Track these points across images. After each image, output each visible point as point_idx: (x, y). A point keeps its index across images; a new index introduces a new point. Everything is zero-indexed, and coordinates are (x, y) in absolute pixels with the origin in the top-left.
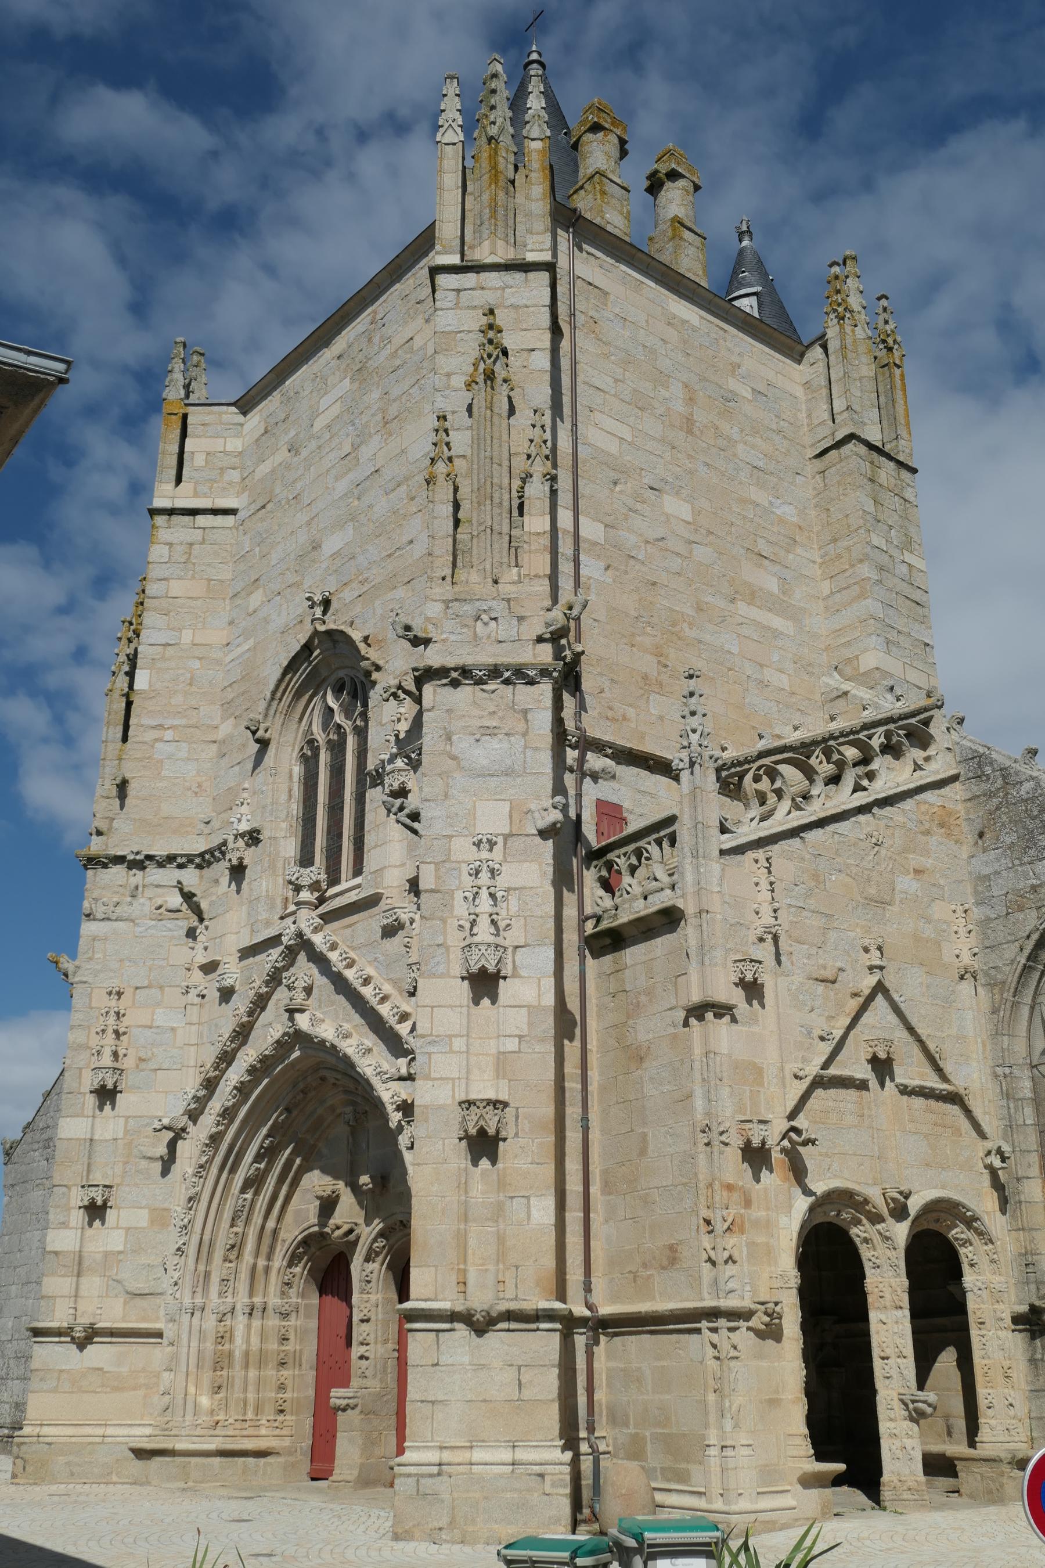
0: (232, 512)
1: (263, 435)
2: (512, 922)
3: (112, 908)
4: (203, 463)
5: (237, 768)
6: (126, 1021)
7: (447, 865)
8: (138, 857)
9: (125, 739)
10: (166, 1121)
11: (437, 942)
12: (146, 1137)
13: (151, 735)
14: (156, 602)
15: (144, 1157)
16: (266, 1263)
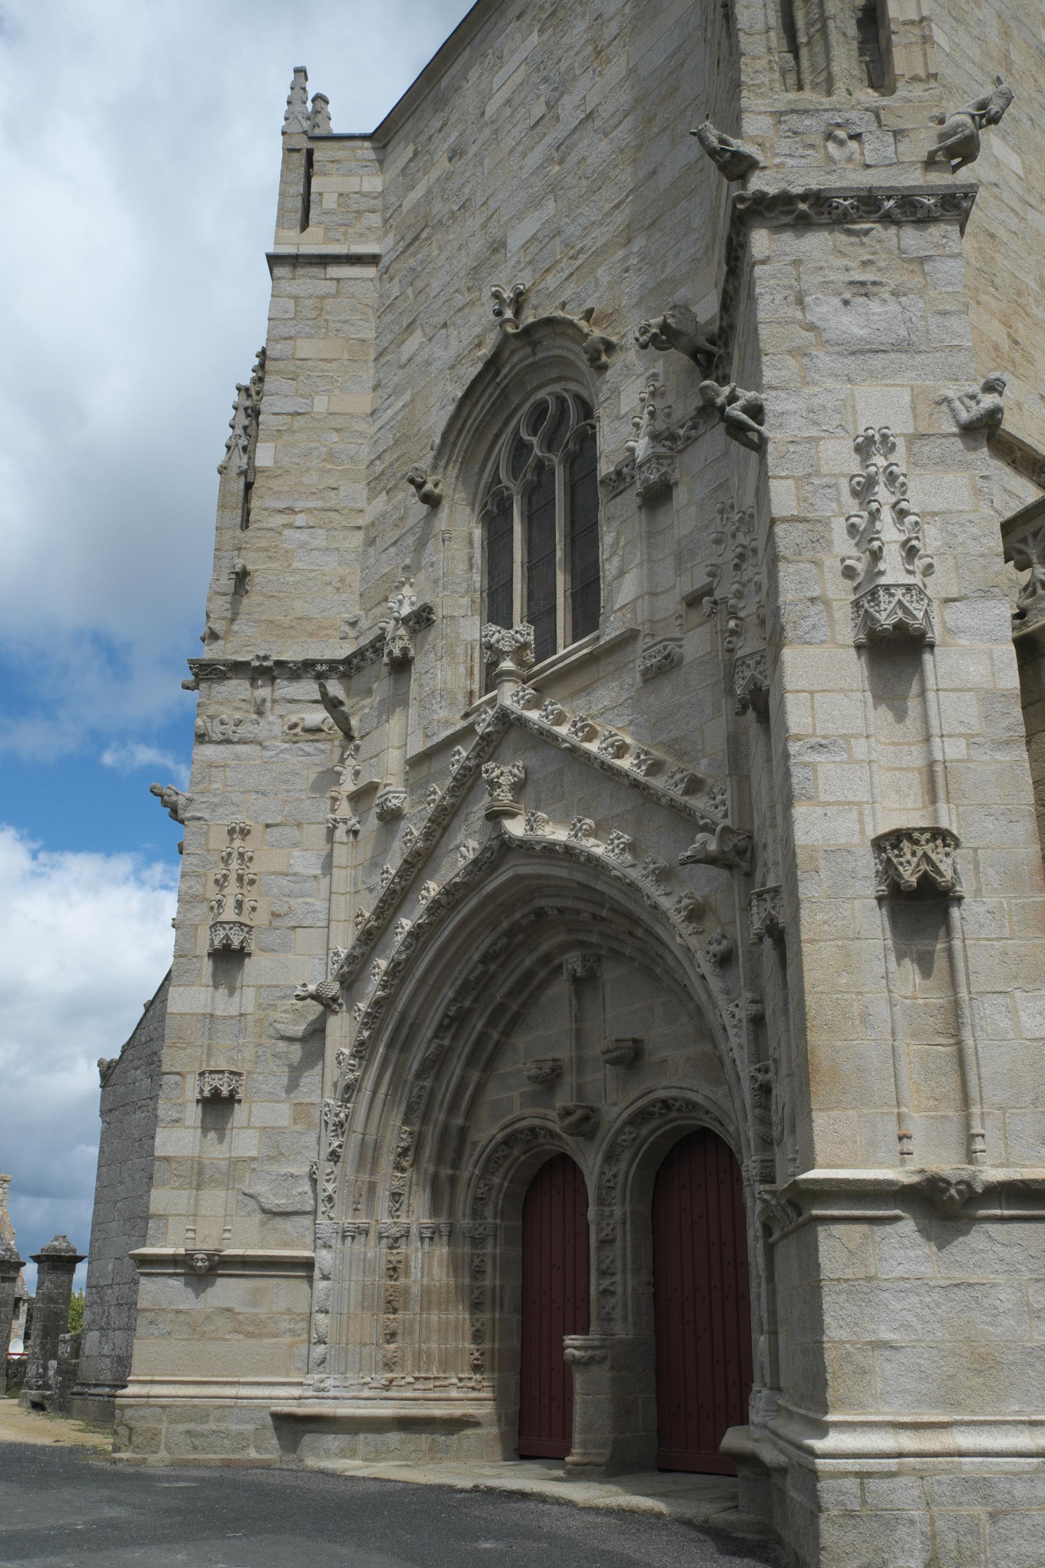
0: (373, 260)
1: (411, 160)
2: (934, 561)
3: (234, 728)
4: (335, 206)
5: (393, 550)
6: (254, 867)
7: (816, 481)
8: (265, 664)
9: (245, 523)
10: (312, 988)
11: (809, 594)
12: (285, 1012)
13: (278, 520)
14: (281, 365)
15: (283, 1038)
16: (449, 1172)
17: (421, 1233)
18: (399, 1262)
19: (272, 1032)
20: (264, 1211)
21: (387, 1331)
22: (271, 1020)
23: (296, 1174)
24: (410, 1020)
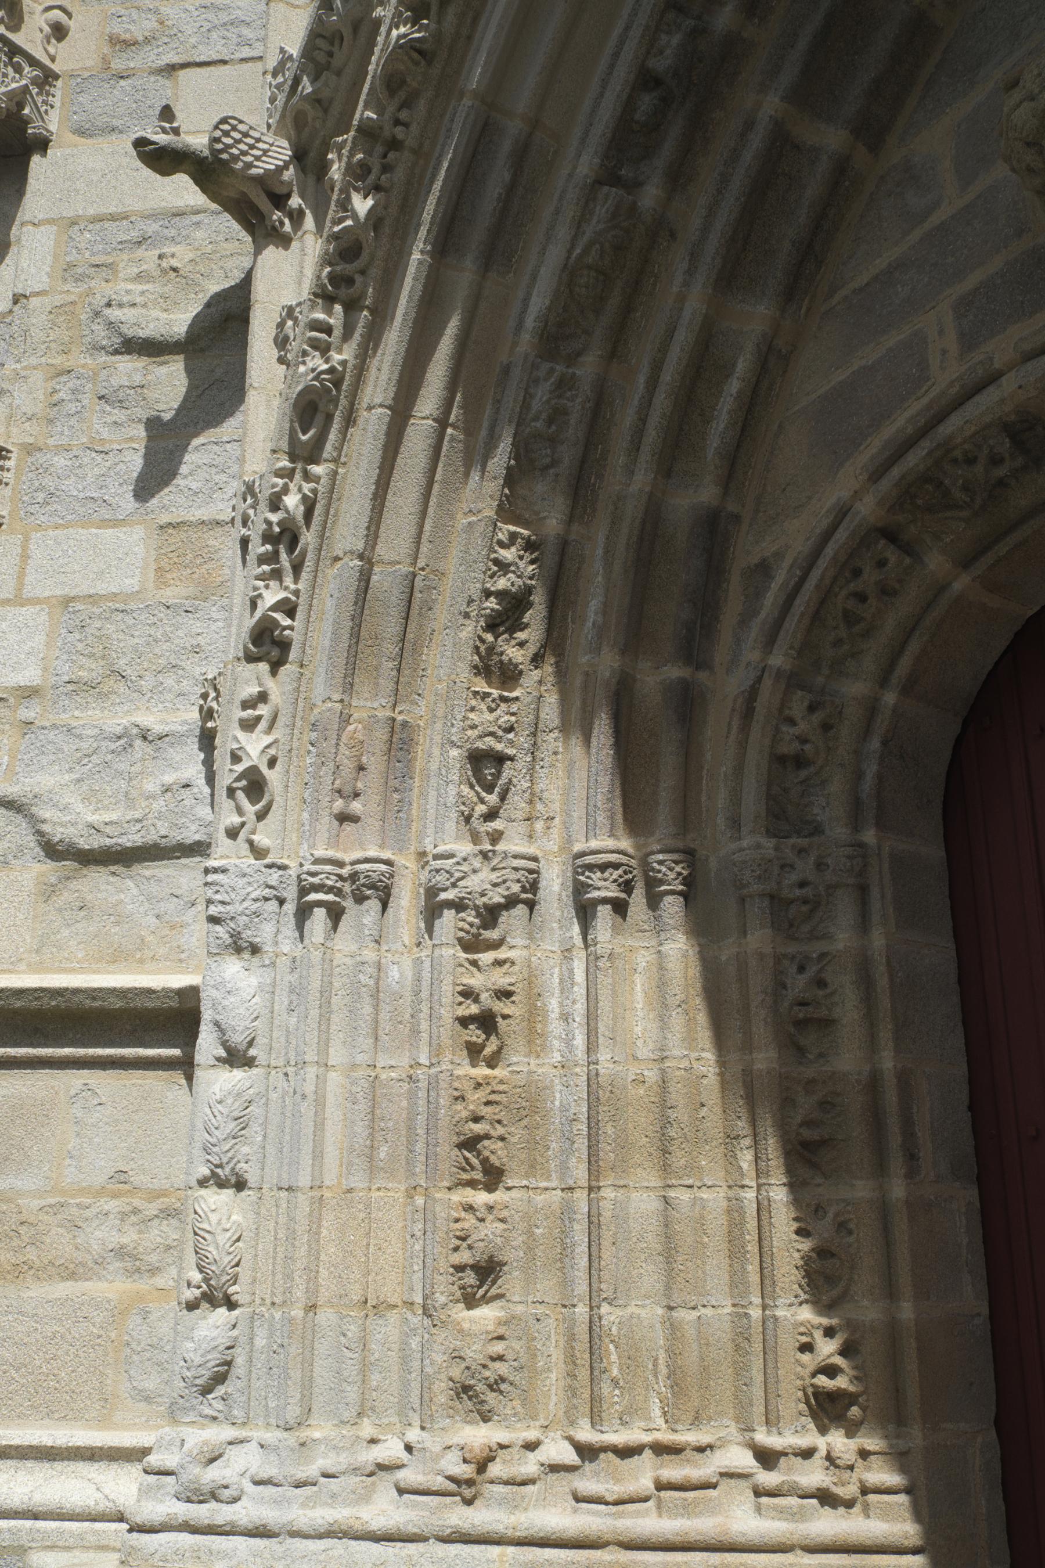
12: (139, 277)
16: (675, 672)
17: (579, 889)
18: (504, 994)
19: (100, 334)
20: (53, 851)
21: (465, 1257)
22: (99, 301)
23: (158, 729)
24: (514, 128)
